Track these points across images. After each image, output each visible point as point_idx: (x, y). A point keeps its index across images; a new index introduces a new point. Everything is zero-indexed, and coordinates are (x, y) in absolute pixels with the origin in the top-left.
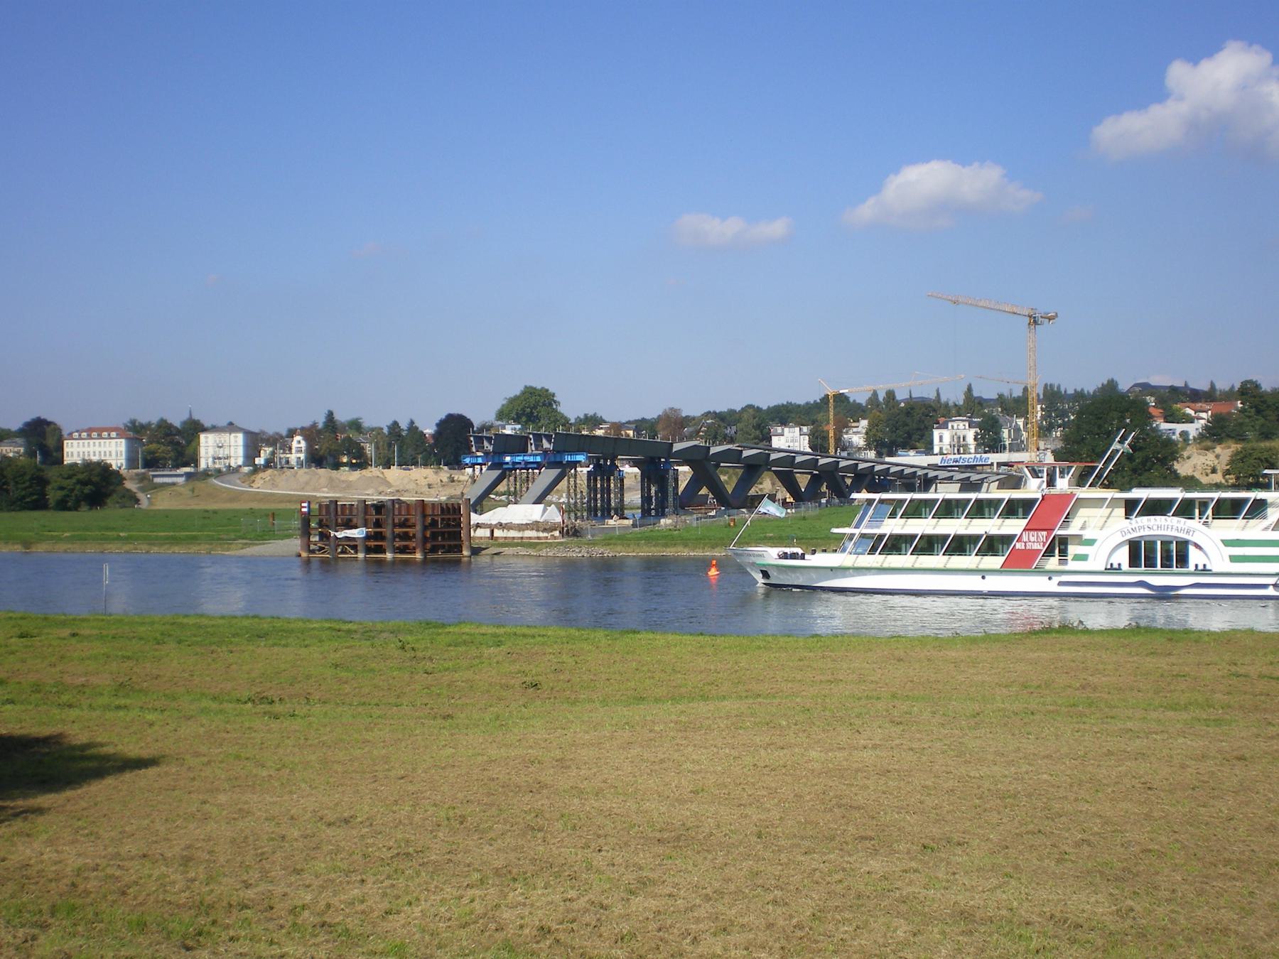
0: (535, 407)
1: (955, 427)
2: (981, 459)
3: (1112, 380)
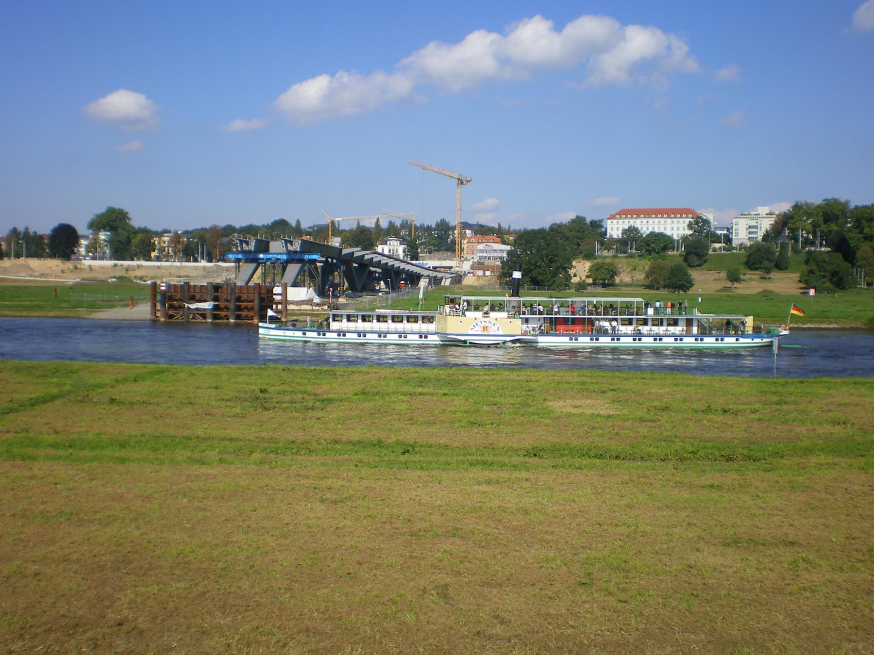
0: (115, 221)
1: (391, 244)
2: (423, 264)
3: (443, 219)
